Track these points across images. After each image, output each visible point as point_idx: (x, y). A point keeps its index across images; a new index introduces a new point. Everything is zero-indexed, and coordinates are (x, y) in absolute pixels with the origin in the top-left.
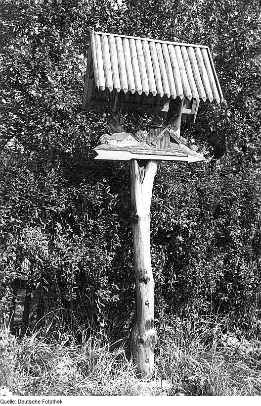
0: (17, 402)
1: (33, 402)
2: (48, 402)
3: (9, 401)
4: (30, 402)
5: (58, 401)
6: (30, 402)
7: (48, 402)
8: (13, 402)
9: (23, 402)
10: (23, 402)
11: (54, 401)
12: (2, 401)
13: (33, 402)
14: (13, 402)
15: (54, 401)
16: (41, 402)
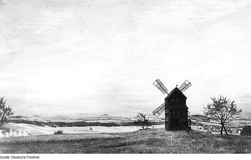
0: (11, 157)
1: (21, 158)
2: (31, 157)
3: (5, 157)
4: (19, 158)
5: (37, 157)
6: (19, 158)
7: (31, 157)
8: (8, 157)
9: (14, 157)
10: (14, 157)
11: (34, 157)
12: (1, 157)
13: (21, 158)
14: (8, 157)
15: (34, 157)
16: (26, 157)
